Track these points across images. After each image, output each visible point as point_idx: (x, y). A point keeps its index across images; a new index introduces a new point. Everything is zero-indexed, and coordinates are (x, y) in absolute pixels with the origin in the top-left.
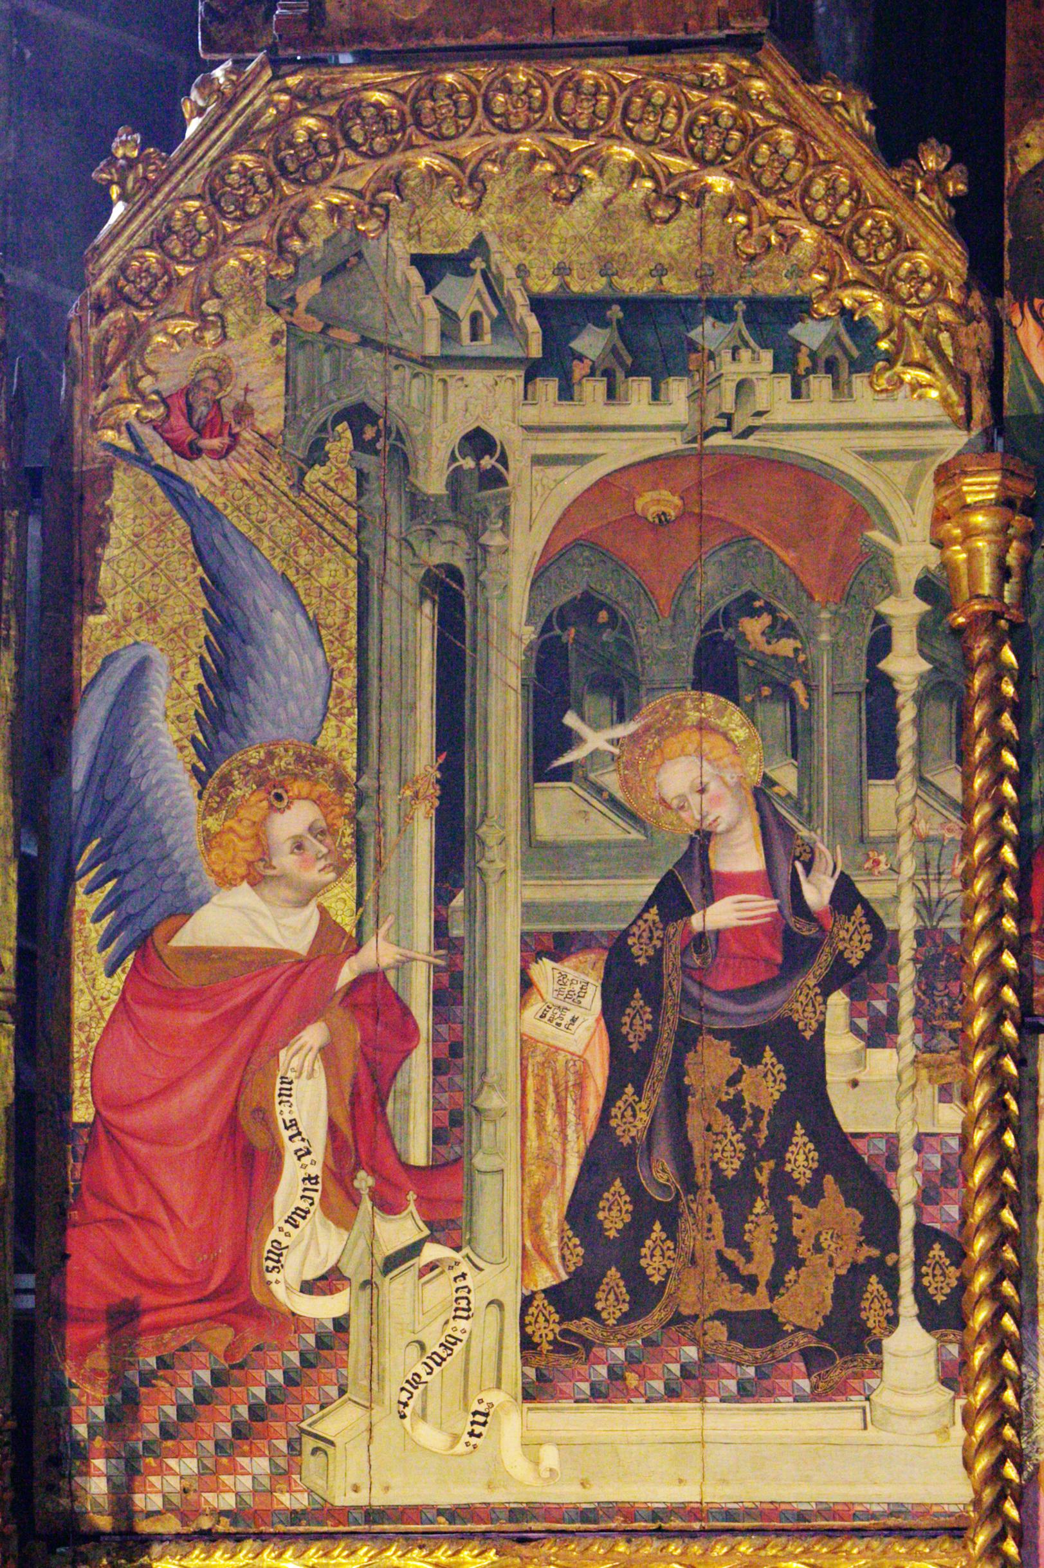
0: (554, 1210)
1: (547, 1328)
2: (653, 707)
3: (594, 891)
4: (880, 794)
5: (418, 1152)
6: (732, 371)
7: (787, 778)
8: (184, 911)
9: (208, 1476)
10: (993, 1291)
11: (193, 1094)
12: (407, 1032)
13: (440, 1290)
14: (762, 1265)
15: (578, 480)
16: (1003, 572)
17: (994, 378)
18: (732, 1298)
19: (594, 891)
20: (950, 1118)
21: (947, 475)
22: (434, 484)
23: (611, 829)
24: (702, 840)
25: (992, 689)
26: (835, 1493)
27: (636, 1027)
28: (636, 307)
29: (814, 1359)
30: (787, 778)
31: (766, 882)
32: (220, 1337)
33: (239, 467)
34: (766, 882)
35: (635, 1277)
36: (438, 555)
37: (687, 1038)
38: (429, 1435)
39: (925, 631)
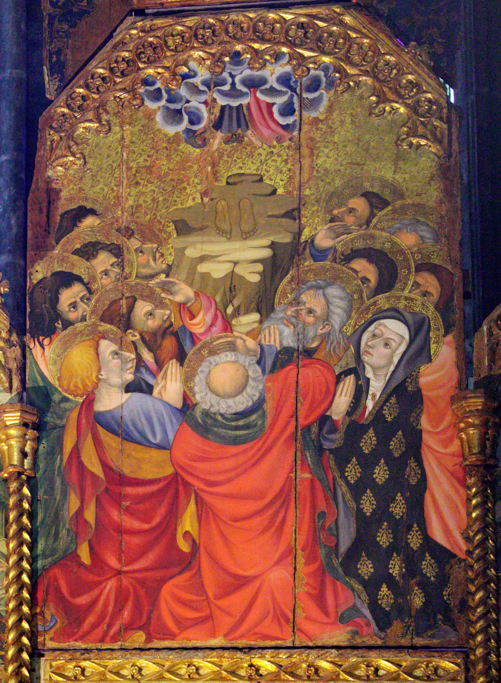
16: (24, 455)
17: (22, 369)
25: (19, 505)
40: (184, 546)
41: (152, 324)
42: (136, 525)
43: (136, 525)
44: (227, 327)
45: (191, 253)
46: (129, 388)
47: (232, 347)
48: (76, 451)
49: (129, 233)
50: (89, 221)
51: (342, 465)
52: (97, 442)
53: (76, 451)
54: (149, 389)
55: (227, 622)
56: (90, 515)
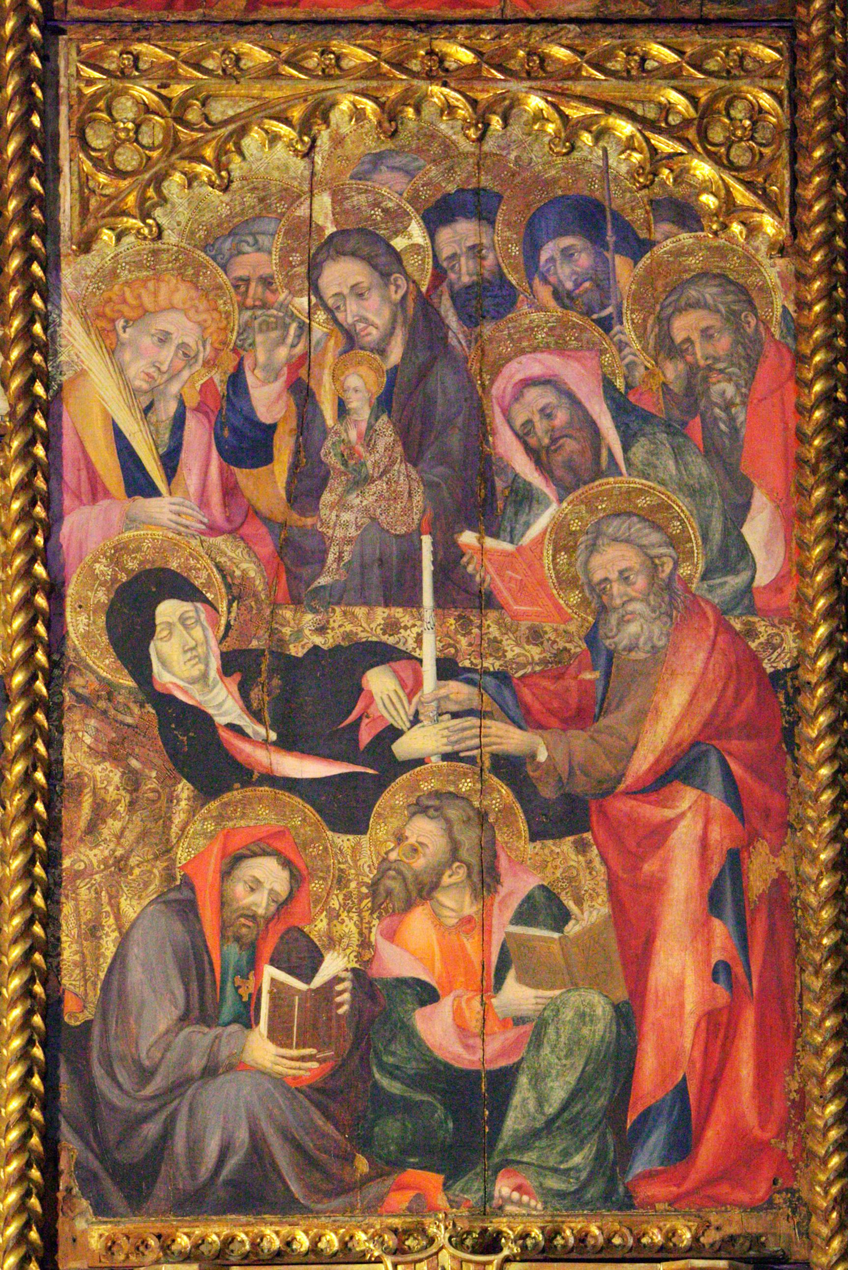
10: (23, 243)
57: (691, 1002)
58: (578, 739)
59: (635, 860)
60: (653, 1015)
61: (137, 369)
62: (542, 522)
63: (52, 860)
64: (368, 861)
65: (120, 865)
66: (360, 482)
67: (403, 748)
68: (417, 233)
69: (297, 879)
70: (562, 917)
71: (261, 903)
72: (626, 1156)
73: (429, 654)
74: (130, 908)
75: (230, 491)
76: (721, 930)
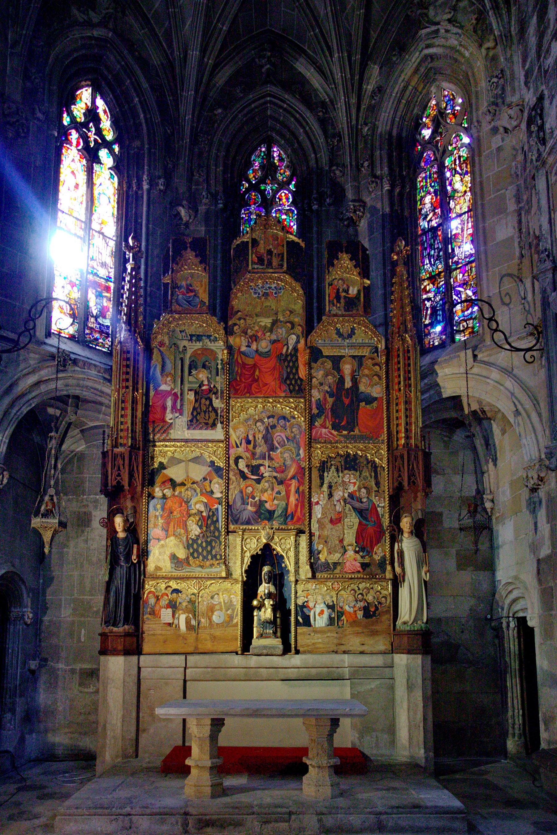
0: (190, 413)
1: (189, 423)
2: (199, 369)
3: (194, 385)
4: (217, 378)
5: (179, 408)
6: (205, 341)
7: (210, 376)
8: (159, 386)
9: (161, 436)
11: (160, 402)
12: (178, 397)
13: (180, 420)
14: (207, 418)
15: (193, 350)
18: (205, 421)
19: (194, 385)
20: (223, 406)
21: (223, 350)
22: (181, 350)
23: (195, 380)
24: (202, 381)
26: (213, 438)
27: (197, 397)
28: (198, 335)
29: (211, 427)
30: (210, 376)
31: (208, 385)
32: (162, 424)
33: (165, 348)
34: (208, 385)
35: (197, 420)
36: (182, 356)
37: (201, 398)
38: (179, 433)
39: (221, 364)
40: (256, 377)
41: (251, 334)
42: (247, 373)
43: (247, 373)
44: (264, 335)
45: (258, 320)
46: (247, 346)
47: (265, 339)
48: (237, 359)
49: (247, 316)
50: (239, 313)
51: (284, 362)
52: (241, 357)
53: (237, 359)
54: (250, 347)
55: (264, 392)
56: (239, 371)
57: (294, 503)
58: (282, 475)
59: (288, 488)
60: (290, 504)
61: (237, 434)
62: (279, 451)
63: (228, 487)
64: (261, 488)
65: (235, 488)
66: (260, 446)
67: (264, 475)
68: (266, 420)
69: (253, 489)
70: (280, 494)
71: (249, 492)
72: (287, 519)
73: (267, 465)
74: (236, 492)
75: (247, 447)
76: (297, 495)
